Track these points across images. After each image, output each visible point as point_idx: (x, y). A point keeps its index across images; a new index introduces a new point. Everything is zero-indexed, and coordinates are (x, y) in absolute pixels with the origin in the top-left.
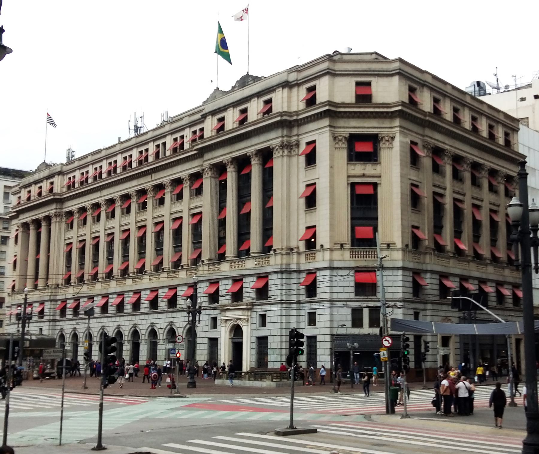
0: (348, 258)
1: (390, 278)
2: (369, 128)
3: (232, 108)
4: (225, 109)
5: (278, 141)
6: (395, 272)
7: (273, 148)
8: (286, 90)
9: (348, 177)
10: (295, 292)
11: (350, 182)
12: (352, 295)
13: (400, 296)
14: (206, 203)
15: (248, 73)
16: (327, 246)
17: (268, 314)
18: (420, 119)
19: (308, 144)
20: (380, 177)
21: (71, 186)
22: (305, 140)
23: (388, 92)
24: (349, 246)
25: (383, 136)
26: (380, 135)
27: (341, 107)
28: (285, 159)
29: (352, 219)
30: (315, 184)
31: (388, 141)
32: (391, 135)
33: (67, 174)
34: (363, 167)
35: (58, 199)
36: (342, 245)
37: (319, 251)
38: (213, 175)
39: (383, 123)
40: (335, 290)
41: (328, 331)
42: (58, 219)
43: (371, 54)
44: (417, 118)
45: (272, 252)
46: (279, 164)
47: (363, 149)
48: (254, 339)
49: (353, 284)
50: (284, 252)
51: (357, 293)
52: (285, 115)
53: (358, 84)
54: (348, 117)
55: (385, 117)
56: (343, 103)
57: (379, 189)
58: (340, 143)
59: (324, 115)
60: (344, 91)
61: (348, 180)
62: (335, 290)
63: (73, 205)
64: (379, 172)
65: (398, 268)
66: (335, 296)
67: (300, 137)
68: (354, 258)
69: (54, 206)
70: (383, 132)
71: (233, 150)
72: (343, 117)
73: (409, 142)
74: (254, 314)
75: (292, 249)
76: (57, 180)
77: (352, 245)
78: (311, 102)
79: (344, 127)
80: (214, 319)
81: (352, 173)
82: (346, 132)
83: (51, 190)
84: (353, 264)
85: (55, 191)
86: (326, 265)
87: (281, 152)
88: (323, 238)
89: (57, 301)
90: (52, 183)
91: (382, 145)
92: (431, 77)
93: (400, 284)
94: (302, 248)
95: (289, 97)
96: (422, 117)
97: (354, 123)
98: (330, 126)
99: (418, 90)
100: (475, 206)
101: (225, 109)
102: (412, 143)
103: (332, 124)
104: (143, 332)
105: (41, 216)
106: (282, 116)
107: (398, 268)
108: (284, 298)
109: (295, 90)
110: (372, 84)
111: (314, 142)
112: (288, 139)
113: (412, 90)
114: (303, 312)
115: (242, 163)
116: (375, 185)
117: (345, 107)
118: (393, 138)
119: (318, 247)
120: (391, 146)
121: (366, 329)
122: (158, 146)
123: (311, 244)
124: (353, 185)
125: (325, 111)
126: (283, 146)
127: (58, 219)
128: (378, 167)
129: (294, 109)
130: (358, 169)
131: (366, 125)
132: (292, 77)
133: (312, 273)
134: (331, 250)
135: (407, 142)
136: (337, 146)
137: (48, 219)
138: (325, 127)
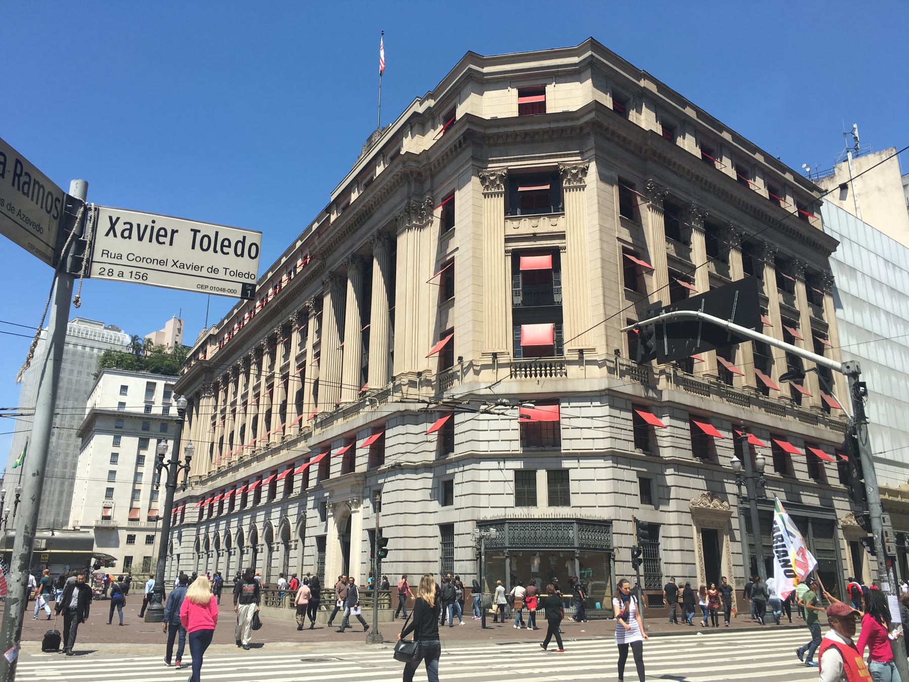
31: (576, 175)
34: (534, 222)
57: (563, 256)
68: (518, 377)
88: (464, 349)
116: (555, 253)
117: (498, 127)
118: (584, 171)
121: (542, 509)
124: (516, 256)
130: (526, 226)
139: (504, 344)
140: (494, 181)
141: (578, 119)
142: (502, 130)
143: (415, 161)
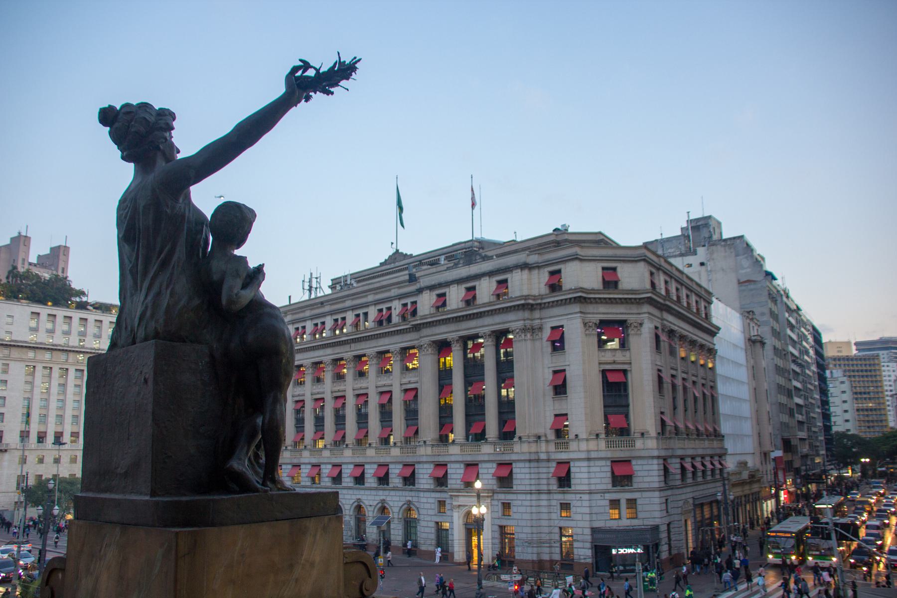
0: (604, 448)
1: (645, 467)
2: (617, 314)
4: (448, 284)
5: (520, 324)
6: (650, 461)
8: (526, 272)
9: (600, 364)
10: (545, 482)
12: (610, 487)
13: (656, 485)
16: (583, 435)
17: (513, 503)
20: (630, 363)
23: (632, 277)
24: (603, 436)
28: (529, 343)
29: (605, 406)
30: (564, 370)
36: (597, 435)
37: (572, 440)
40: (593, 481)
41: (587, 525)
45: (516, 439)
48: (497, 528)
50: (531, 439)
51: (614, 484)
53: (603, 269)
62: (593, 481)
65: (653, 457)
66: (593, 487)
70: (631, 318)
71: (460, 328)
72: (591, 303)
75: (539, 437)
77: (607, 433)
79: (593, 313)
80: (442, 503)
82: (597, 318)
84: (609, 455)
86: (583, 455)
93: (656, 473)
94: (551, 436)
97: (602, 309)
98: (581, 312)
100: (684, 379)
101: (448, 284)
104: (347, 507)
106: (525, 299)
107: (653, 457)
108: (533, 488)
109: (535, 272)
114: (554, 503)
116: (625, 372)
118: (641, 324)
119: (572, 436)
122: (358, 316)
123: (560, 433)
124: (604, 372)
126: (524, 330)
129: (535, 292)
131: (614, 311)
132: (533, 259)
133: (564, 465)
134: (587, 440)
138: (576, 313)
139: (600, 426)
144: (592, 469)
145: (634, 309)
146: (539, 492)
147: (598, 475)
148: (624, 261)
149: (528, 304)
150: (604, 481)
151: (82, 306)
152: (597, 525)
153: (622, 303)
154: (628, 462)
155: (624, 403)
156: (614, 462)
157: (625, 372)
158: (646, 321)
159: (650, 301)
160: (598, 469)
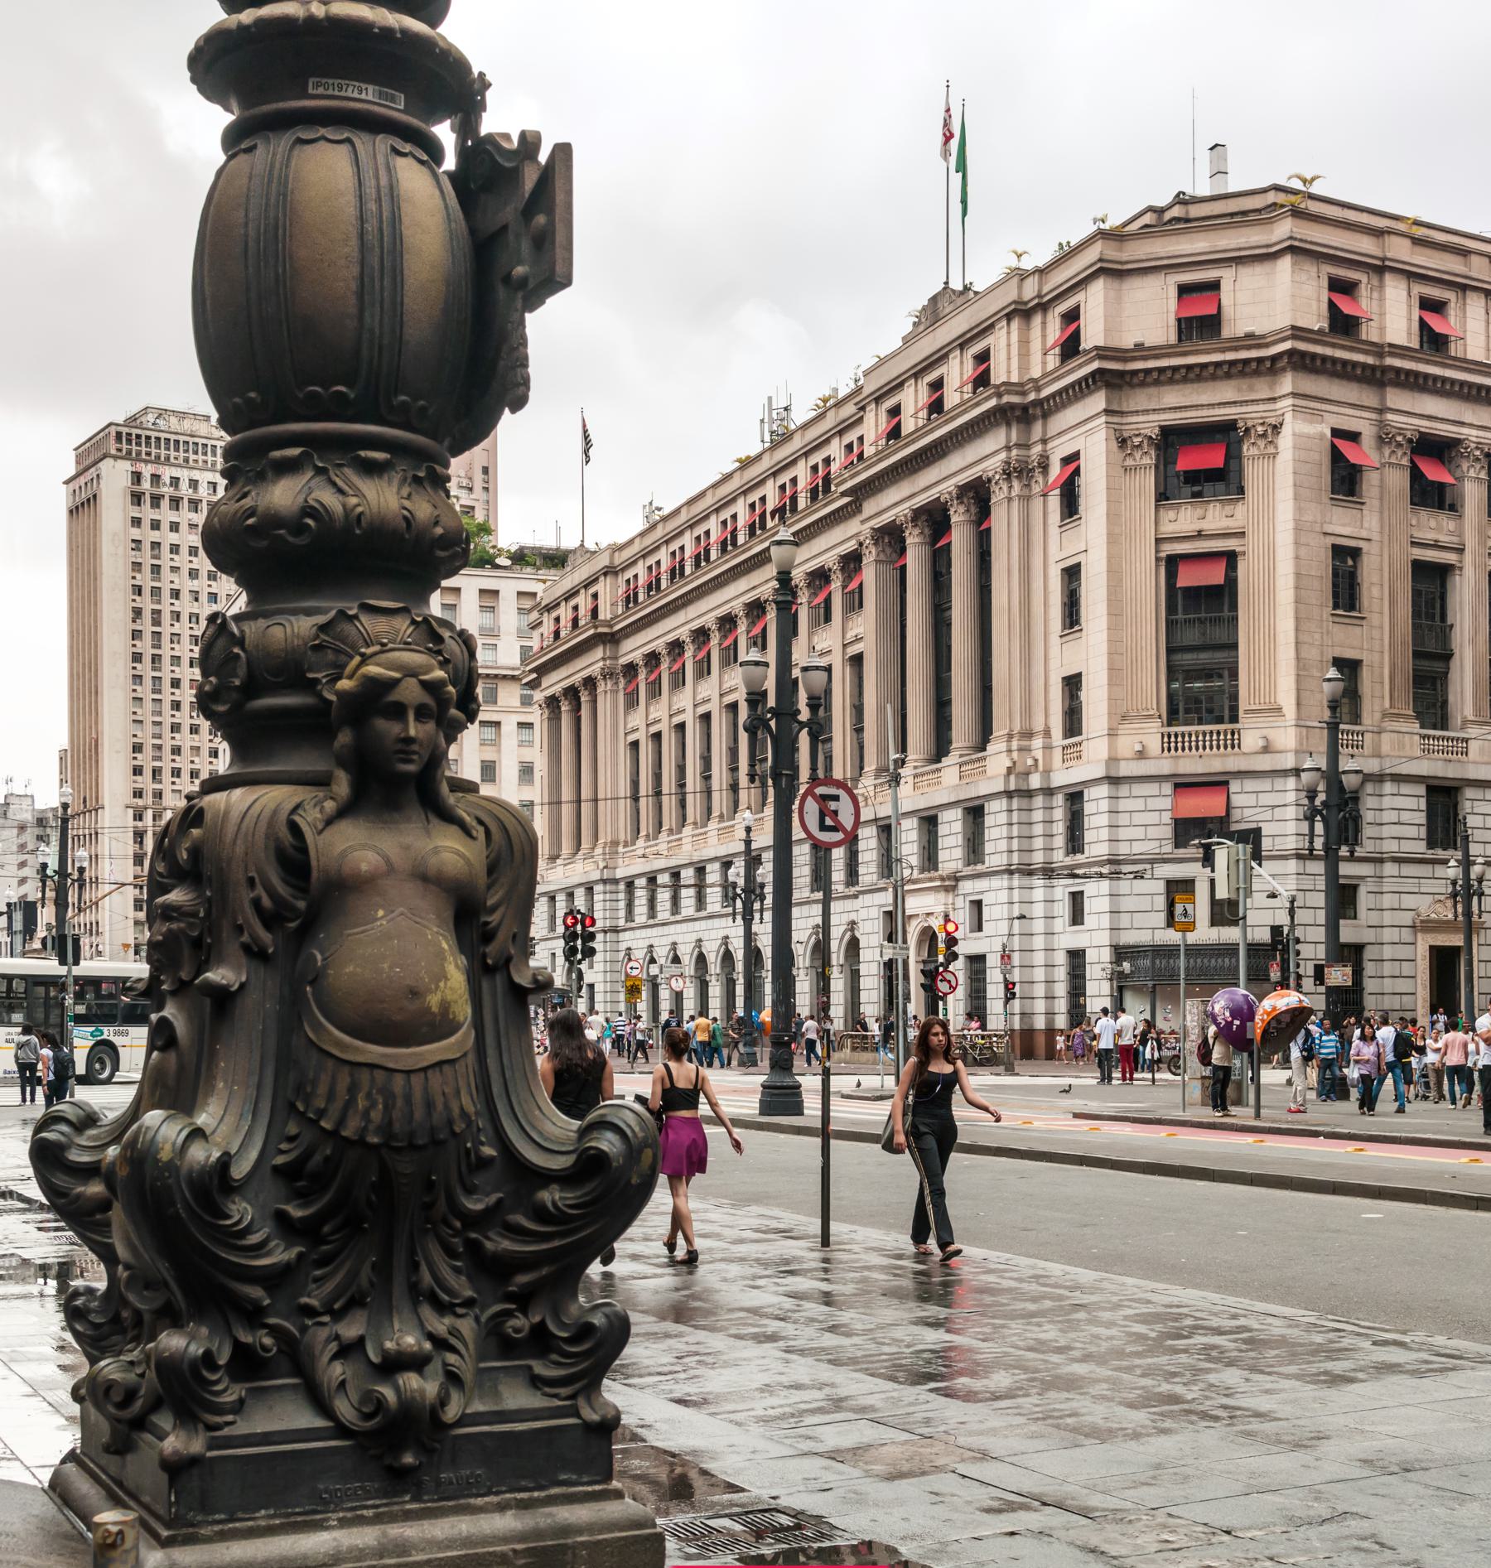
1: (1266, 799)
2: (1212, 406)
3: (913, 381)
6: (1279, 783)
7: (989, 480)
9: (1158, 541)
11: (1163, 555)
12: (1168, 848)
14: (865, 627)
15: (946, 283)
18: (1364, 366)
19: (1066, 461)
21: (631, 599)
22: (1059, 451)
23: (1271, 301)
25: (1250, 424)
26: (1241, 424)
27: (1134, 359)
32: (1273, 421)
33: (623, 570)
34: (1199, 512)
35: (605, 634)
38: (882, 557)
39: (1251, 389)
42: (609, 686)
43: (1265, 191)
44: (1355, 364)
46: (1003, 521)
47: (1199, 462)
49: (1167, 817)
52: (1009, 392)
53: (1184, 290)
54: (1157, 383)
55: (1257, 373)
56: (1139, 346)
58: (1138, 455)
59: (1094, 382)
60: (1144, 315)
61: (1157, 551)
63: (633, 649)
64: (1240, 524)
67: (1050, 446)
69: (599, 653)
72: (1143, 384)
73: (1328, 433)
74: (960, 902)
76: (603, 587)
78: (1070, 348)
81: (1168, 529)
82: (1148, 425)
83: (595, 612)
84: (1165, 766)
85: (601, 617)
87: (1005, 488)
89: (616, 881)
90: (595, 596)
91: (1248, 450)
92: (1407, 242)
95: (1024, 342)
96: (1370, 360)
97: (1172, 396)
98: (1107, 412)
99: (1363, 286)
102: (1336, 433)
103: (1115, 407)
105: (577, 679)
110: (1225, 287)
111: (1075, 456)
112: (1023, 452)
113: (1342, 287)
115: (934, 519)
116: (1231, 558)
117: (1145, 358)
118: (1277, 428)
120: (1271, 450)
124: (1172, 564)
125: (1093, 374)
127: (609, 686)
128: (1240, 509)
130: (1185, 519)
131: (1204, 399)
135: (1322, 436)
136: (1129, 462)
137: (590, 682)
140: (1140, 446)
141: (1267, 345)
142: (1151, 364)
143: (1017, 393)
144: (1124, 805)
145: (1261, 388)
146: (1028, 872)
147: (1139, 818)
148: (1239, 261)
149: (1012, 407)
150: (1153, 832)
151: (487, 561)
152: (1129, 938)
153: (1228, 376)
154: (1218, 783)
155: (1224, 640)
156: (1183, 785)
157: (1231, 558)
158: (1288, 417)
159: (1301, 362)
160: (1138, 804)
